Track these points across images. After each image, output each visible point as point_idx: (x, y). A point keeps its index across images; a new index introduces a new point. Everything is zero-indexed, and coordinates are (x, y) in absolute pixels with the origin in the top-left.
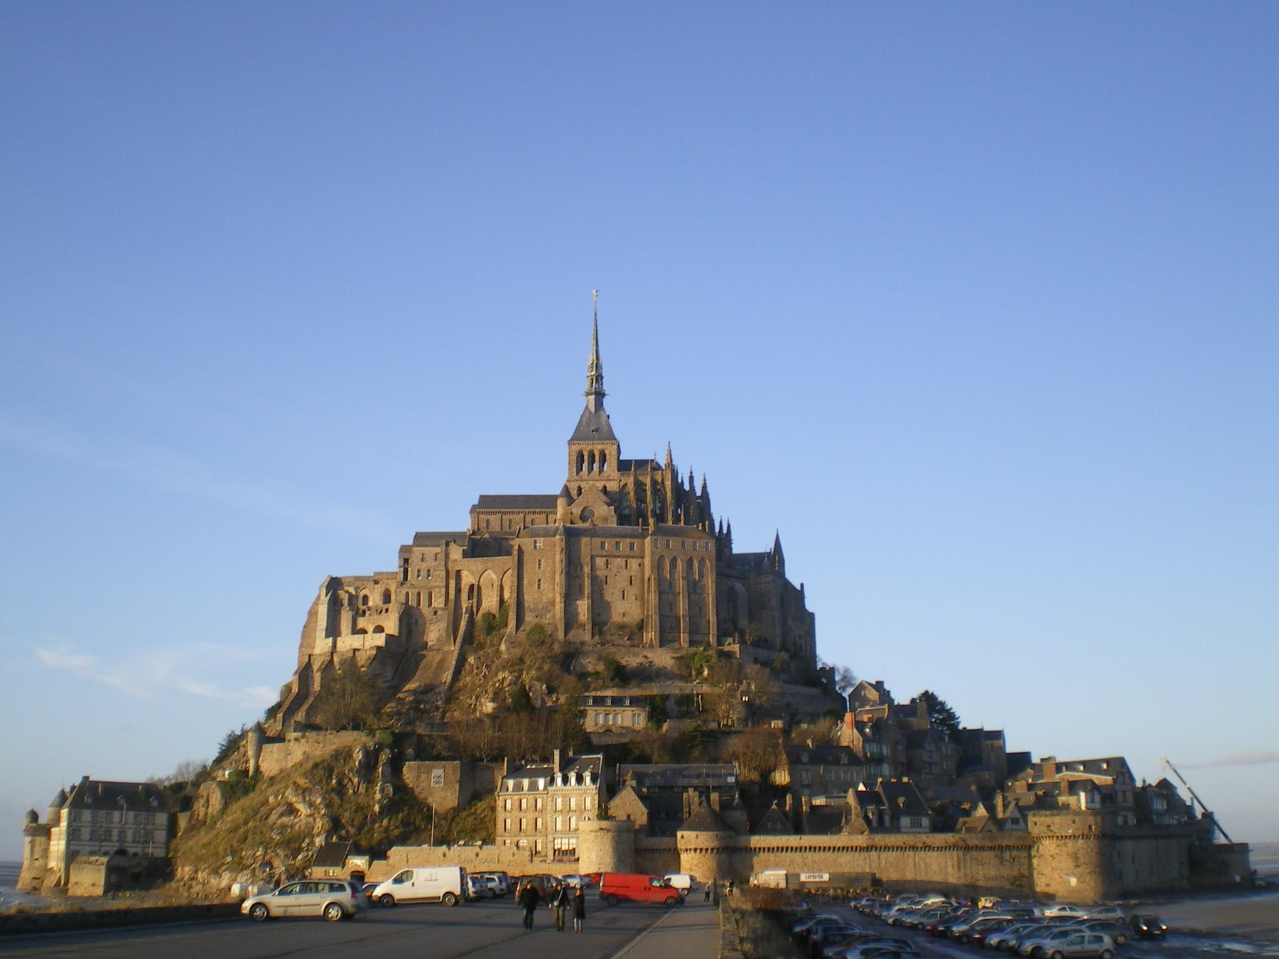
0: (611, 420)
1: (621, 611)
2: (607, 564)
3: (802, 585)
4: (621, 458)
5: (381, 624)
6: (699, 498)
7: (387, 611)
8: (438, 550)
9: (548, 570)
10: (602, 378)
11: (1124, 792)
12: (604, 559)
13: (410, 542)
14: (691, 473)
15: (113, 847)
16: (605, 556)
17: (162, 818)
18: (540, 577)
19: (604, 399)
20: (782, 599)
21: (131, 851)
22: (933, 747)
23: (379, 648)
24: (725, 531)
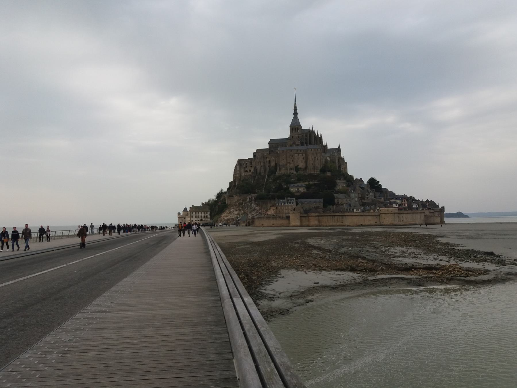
2: (298, 155)
3: (344, 156)
5: (250, 169)
7: (251, 166)
10: (297, 110)
11: (405, 204)
13: (256, 151)
15: (199, 219)
17: (209, 213)
20: (338, 160)
21: (203, 220)
22: (368, 194)
23: (250, 175)
24: (326, 145)
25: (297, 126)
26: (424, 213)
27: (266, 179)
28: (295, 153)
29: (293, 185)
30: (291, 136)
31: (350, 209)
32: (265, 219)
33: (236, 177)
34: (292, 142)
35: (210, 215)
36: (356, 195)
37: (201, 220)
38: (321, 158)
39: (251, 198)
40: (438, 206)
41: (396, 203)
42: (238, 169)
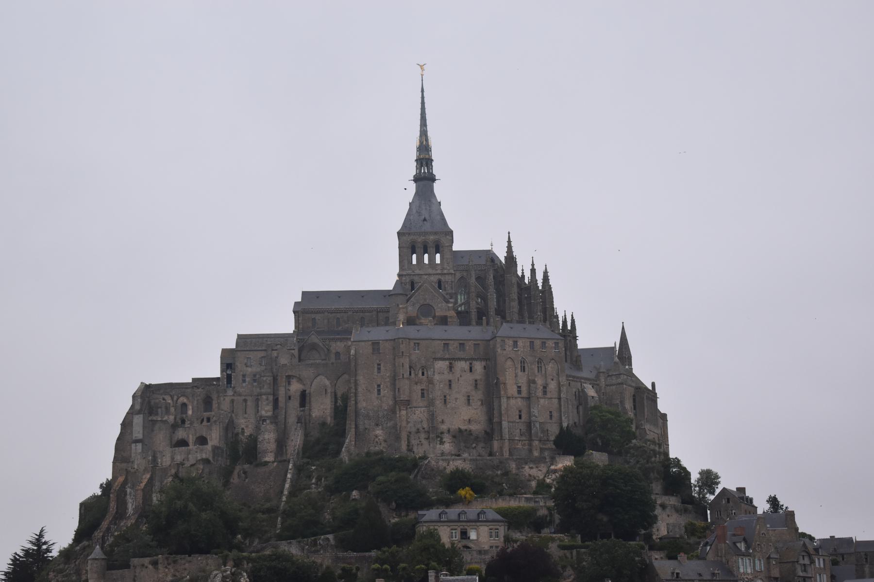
0: (443, 208)
1: (465, 419)
2: (451, 367)
3: (653, 385)
4: (456, 247)
6: (541, 291)
7: (208, 420)
8: (263, 354)
9: (387, 375)
10: (432, 160)
12: (447, 363)
14: (533, 265)
16: (447, 359)
18: (379, 383)
19: (434, 184)
22: (807, 561)
23: (206, 461)
24: (569, 328)
25: (436, 233)
27: (287, 486)
28: (436, 359)
29: (440, 511)
30: (407, 279)
33: (127, 472)
34: (417, 306)
36: (760, 565)
38: (559, 386)
39: (233, 574)
42: (138, 432)
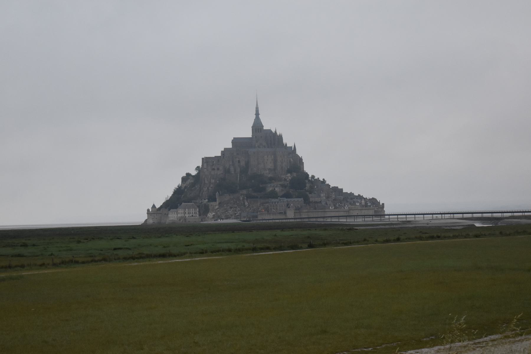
2: (268, 157)
3: (302, 157)
7: (219, 164)
13: (223, 150)
15: (191, 215)
17: (198, 209)
21: (194, 215)
22: (331, 193)
26: (374, 209)
31: (327, 207)
32: (266, 215)
35: (199, 212)
36: (324, 195)
37: (192, 216)
40: (379, 202)
41: (358, 202)
